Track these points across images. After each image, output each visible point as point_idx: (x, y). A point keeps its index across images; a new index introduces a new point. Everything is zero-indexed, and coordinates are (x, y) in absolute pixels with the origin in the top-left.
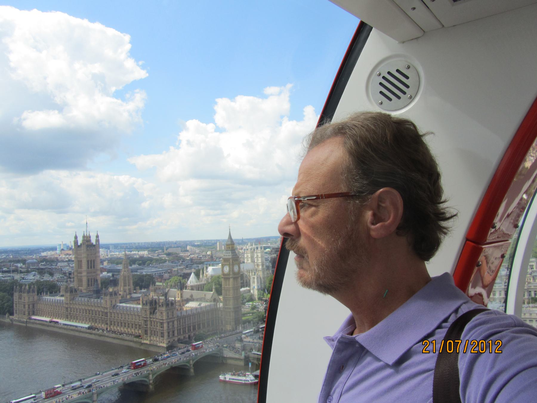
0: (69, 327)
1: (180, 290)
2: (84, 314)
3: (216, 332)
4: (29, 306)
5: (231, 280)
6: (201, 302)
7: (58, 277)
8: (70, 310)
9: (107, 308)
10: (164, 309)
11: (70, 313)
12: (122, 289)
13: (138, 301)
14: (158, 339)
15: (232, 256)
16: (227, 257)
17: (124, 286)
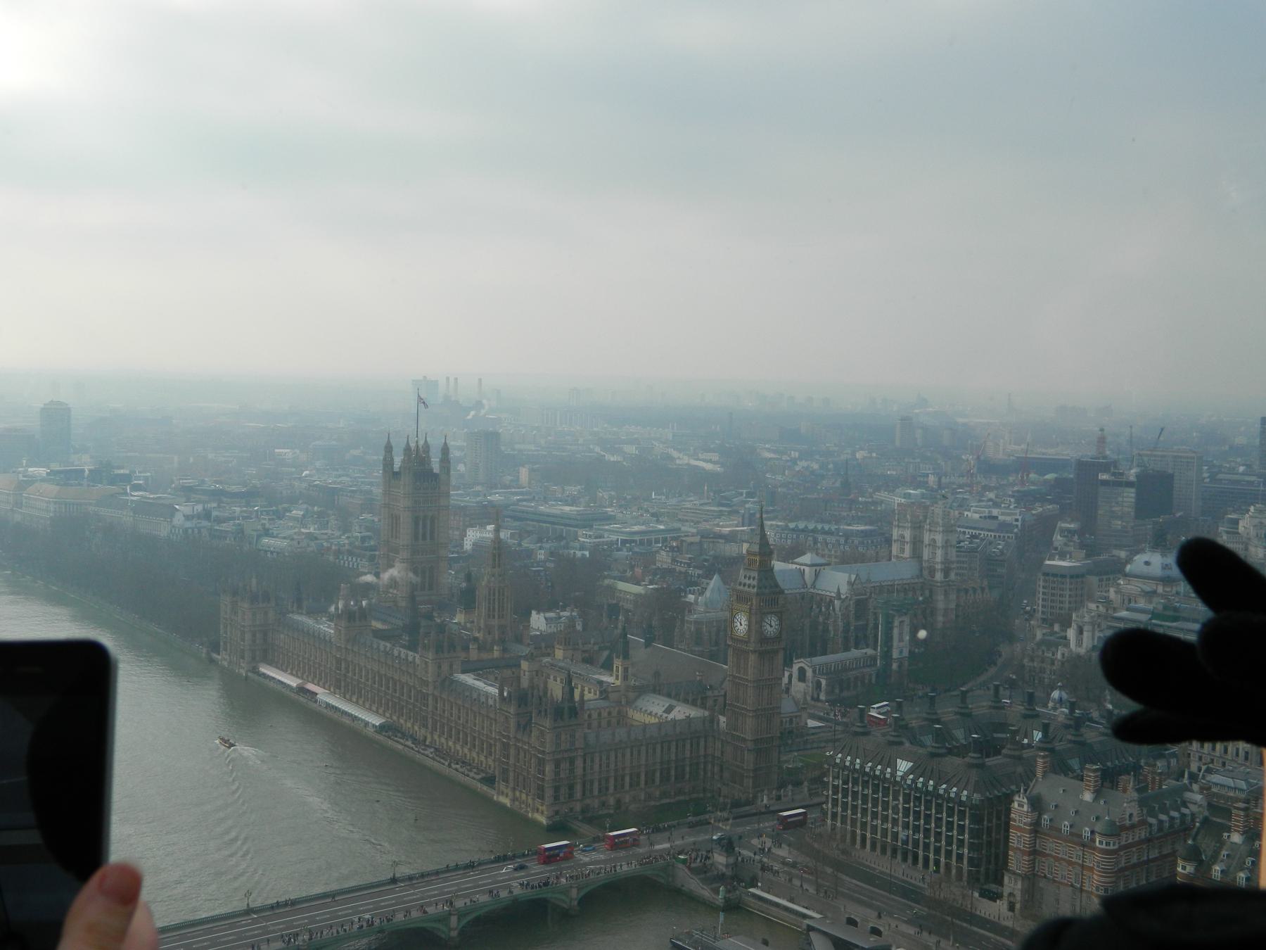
0: (336, 716)
1: (621, 657)
2: (376, 686)
3: (701, 795)
4: (254, 635)
5: (752, 658)
6: (674, 702)
7: (357, 537)
8: (346, 668)
9: (426, 683)
10: (547, 723)
11: (345, 675)
12: (482, 626)
13: (514, 670)
14: (530, 801)
15: (759, 588)
16: (746, 588)
17: (489, 616)
